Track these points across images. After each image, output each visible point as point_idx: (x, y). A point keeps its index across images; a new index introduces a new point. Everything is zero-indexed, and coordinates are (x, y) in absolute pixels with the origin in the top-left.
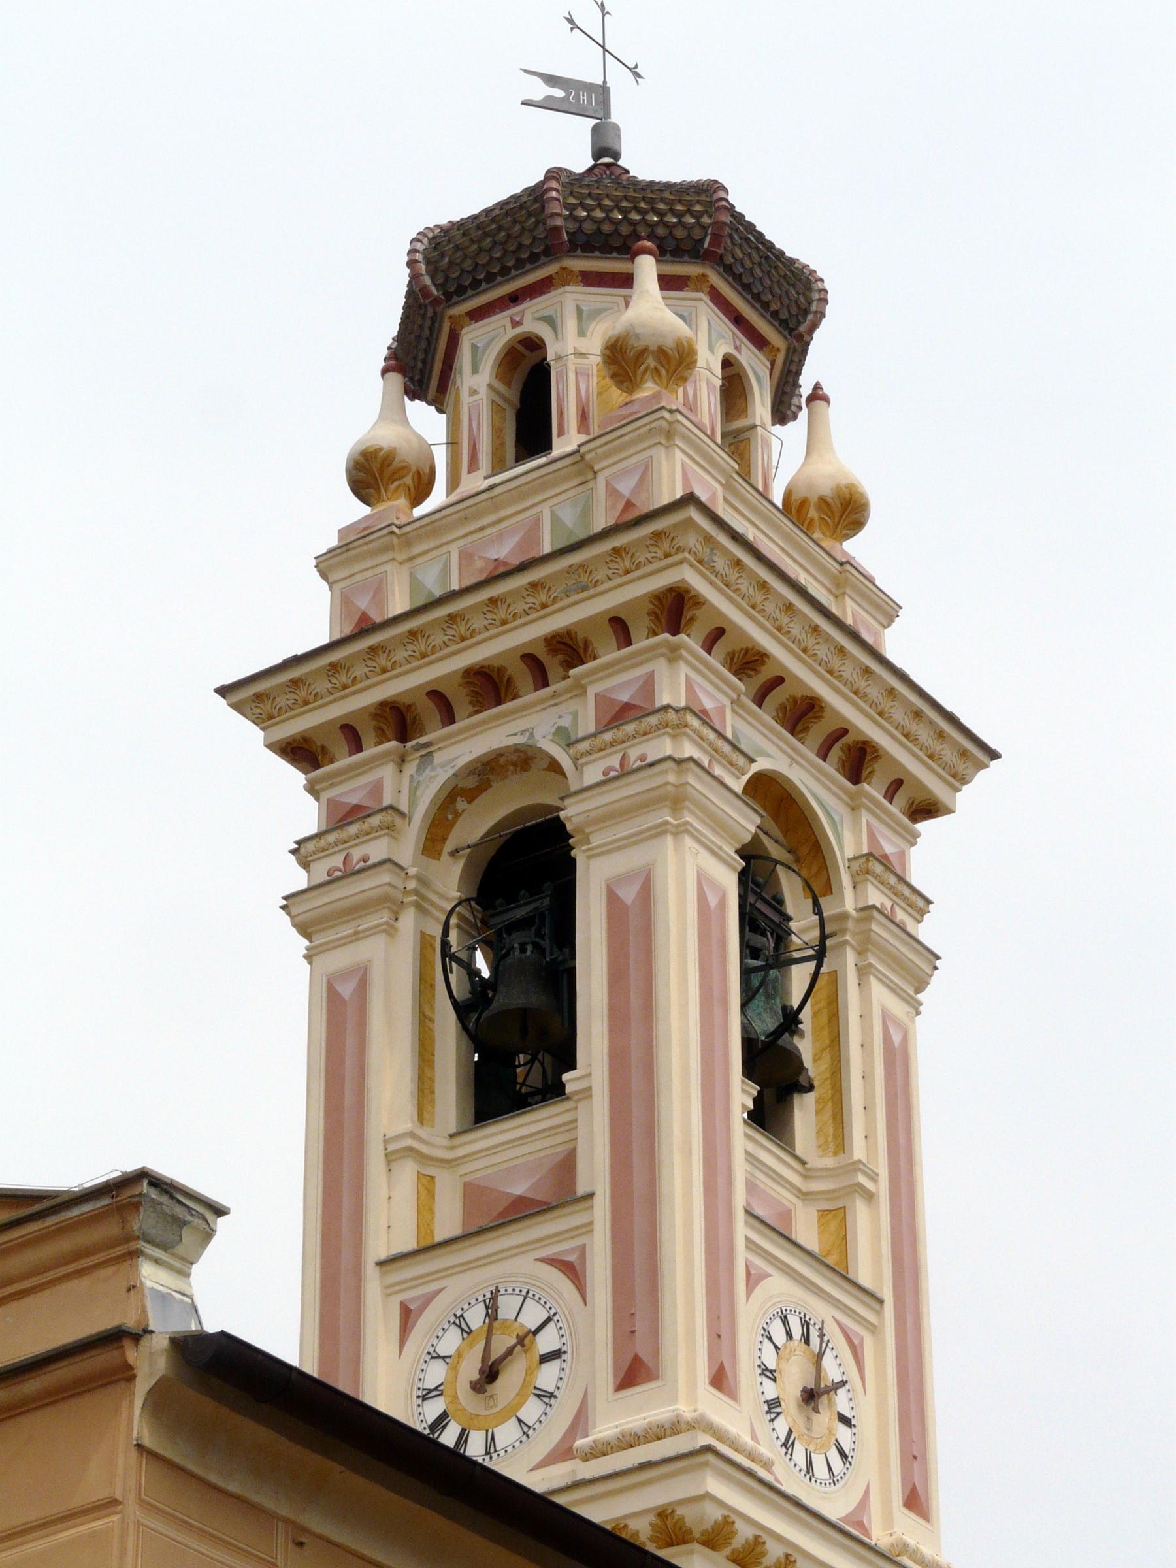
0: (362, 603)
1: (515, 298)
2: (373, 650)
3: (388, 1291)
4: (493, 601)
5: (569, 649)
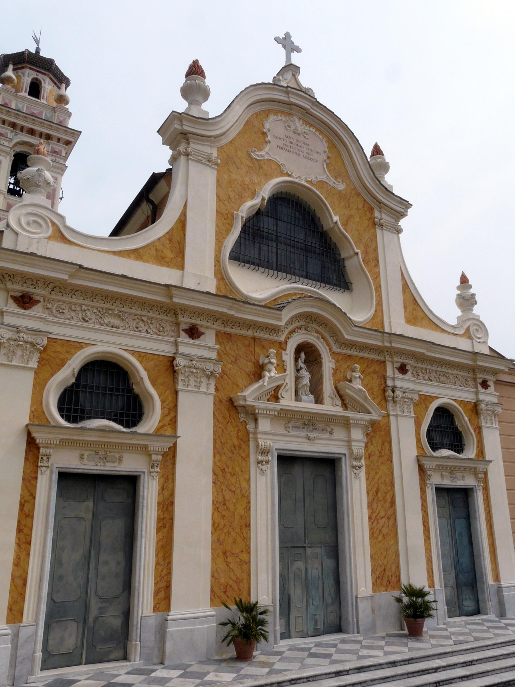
0: (7, 101)
1: (38, 71)
4: (42, 122)
5: (48, 137)
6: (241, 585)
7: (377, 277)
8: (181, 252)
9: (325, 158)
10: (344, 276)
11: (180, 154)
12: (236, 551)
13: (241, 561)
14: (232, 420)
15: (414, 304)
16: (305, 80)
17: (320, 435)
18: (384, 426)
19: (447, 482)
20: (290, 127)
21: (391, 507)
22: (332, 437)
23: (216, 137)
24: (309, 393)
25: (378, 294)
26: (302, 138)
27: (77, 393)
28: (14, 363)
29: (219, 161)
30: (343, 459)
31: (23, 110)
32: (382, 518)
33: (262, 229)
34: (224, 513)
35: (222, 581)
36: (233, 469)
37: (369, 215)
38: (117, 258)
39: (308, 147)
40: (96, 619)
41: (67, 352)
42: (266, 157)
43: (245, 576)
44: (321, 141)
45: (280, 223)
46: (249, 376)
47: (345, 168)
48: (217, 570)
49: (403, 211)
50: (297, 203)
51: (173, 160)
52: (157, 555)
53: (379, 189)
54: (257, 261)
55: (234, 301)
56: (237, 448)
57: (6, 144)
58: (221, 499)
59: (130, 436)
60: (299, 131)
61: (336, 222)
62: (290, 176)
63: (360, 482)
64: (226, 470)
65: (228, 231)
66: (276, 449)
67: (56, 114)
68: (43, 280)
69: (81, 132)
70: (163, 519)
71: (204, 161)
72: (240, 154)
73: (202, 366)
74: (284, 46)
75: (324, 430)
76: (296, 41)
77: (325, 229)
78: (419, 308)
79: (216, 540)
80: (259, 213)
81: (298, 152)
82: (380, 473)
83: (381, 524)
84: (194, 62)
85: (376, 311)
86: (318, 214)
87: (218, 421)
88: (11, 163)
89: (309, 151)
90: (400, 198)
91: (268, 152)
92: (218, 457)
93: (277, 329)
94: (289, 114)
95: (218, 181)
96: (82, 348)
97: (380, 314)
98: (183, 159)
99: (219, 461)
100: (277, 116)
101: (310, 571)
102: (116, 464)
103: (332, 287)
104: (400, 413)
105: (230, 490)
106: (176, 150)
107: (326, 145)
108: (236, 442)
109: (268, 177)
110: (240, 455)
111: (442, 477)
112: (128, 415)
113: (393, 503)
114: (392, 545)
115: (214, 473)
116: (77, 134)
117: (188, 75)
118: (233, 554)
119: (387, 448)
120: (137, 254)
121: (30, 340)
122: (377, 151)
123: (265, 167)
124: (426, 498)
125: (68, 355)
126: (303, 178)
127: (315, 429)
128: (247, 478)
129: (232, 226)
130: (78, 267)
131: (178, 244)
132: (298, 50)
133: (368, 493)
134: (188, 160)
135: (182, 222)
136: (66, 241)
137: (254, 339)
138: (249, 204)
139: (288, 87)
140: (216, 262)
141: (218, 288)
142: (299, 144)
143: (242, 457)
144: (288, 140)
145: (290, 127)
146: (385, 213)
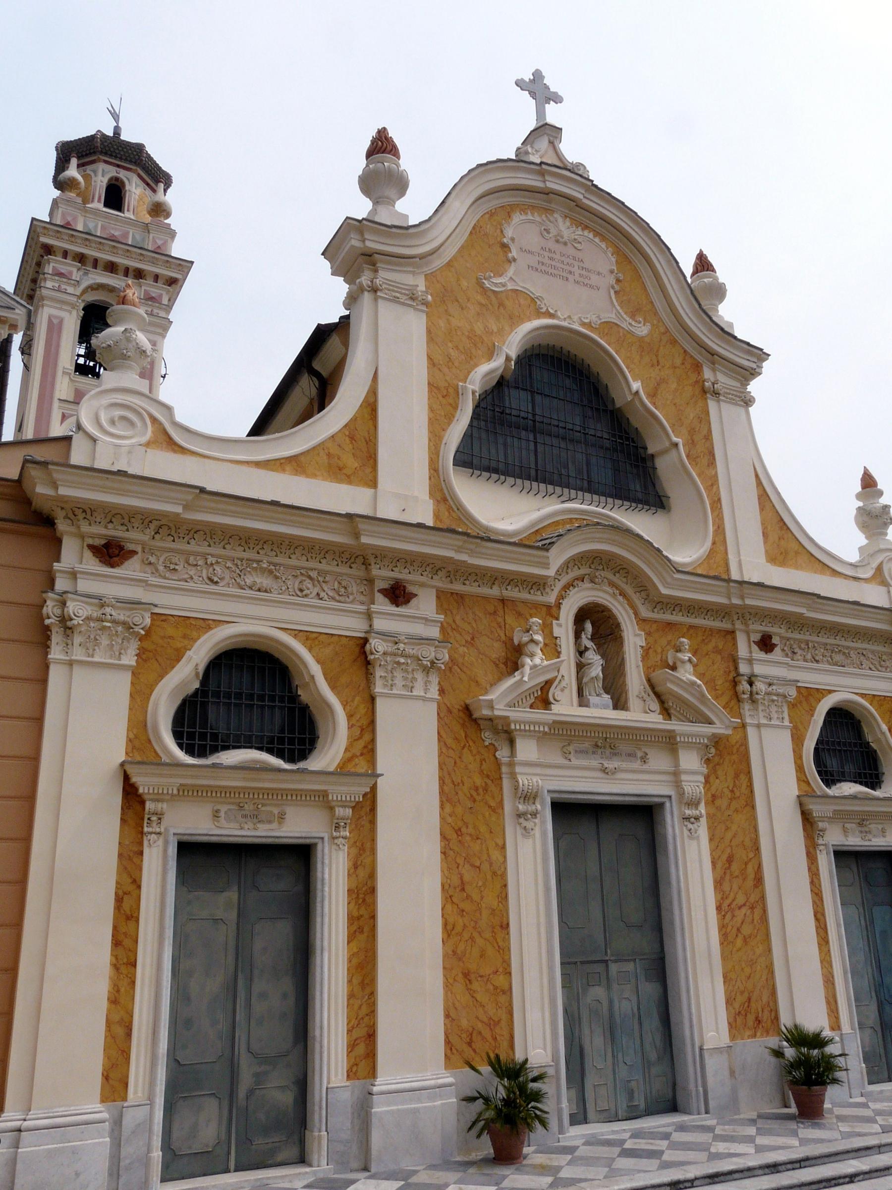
0: (69, 219)
1: (118, 166)
2: (87, 239)
3: (60, 408)
5: (139, 274)
6: (497, 1030)
7: (713, 483)
8: (370, 457)
9: (612, 281)
10: (654, 485)
11: (362, 289)
12: (486, 970)
13: (496, 988)
14: (471, 743)
15: (781, 529)
16: (571, 150)
17: (624, 765)
18: (738, 746)
19: (855, 841)
20: (548, 233)
21: (756, 886)
22: (645, 767)
23: (422, 257)
24: (602, 691)
25: (716, 513)
26: (571, 251)
27: (204, 705)
28: (97, 659)
29: (429, 297)
30: (668, 805)
31: (96, 231)
32: (740, 908)
33: (508, 411)
34: (462, 905)
35: (464, 1023)
36: (475, 827)
37: (694, 377)
38: (262, 473)
39: (581, 264)
40: (251, 1092)
41: (185, 636)
42: (510, 286)
43: (504, 1017)
44: (605, 253)
45: (538, 398)
46: (497, 665)
47: (648, 295)
48: (454, 1004)
49: (754, 366)
50: (566, 363)
51: (351, 300)
52: (350, 982)
53: (710, 330)
54: (501, 466)
55: (465, 538)
56: (481, 790)
57: (70, 290)
58: (456, 881)
59: (297, 777)
60: (566, 238)
61: (637, 392)
62: (552, 316)
63: (699, 846)
64: (464, 830)
65: (450, 418)
66: (549, 791)
67: (151, 235)
68: (140, 516)
69: (192, 263)
70: (359, 918)
71: (403, 299)
72: (464, 284)
73: (414, 651)
74: (533, 94)
76: (553, 83)
77: (619, 404)
78: (790, 535)
79: (451, 953)
80: (501, 384)
81: (565, 274)
82: (734, 827)
83: (739, 919)
84: (379, 132)
85: (714, 543)
86: (605, 379)
87: (445, 744)
88: (79, 322)
89: (584, 272)
90: (748, 344)
91: (513, 278)
92: (448, 808)
93: (542, 582)
94: (547, 211)
95: (429, 331)
96: (210, 628)
97: (722, 548)
98: (367, 297)
99: (450, 815)
100: (527, 214)
102: (275, 825)
103: (634, 505)
104: (764, 721)
105: (473, 866)
106: (355, 284)
107: (614, 260)
108: (479, 781)
109: (515, 320)
110: (486, 803)
111: (845, 831)
112: (291, 741)
113: (759, 880)
114: (760, 956)
115: (444, 837)
116: (185, 266)
117: (370, 154)
118: (481, 976)
120: (295, 464)
121: (122, 618)
122: (703, 264)
123: (509, 304)
124: (818, 870)
125: (186, 642)
126: (575, 318)
127: (615, 754)
128: (500, 843)
129: (455, 408)
130: (198, 491)
131: (364, 444)
132: (557, 99)
133: (714, 863)
134: (376, 299)
135: (370, 407)
136: (176, 448)
137: (503, 601)
138: (484, 368)
139: (542, 163)
140: (432, 472)
141: (437, 516)
142: (566, 261)
143: (490, 807)
144: (546, 254)
145: (548, 233)
146: (722, 372)
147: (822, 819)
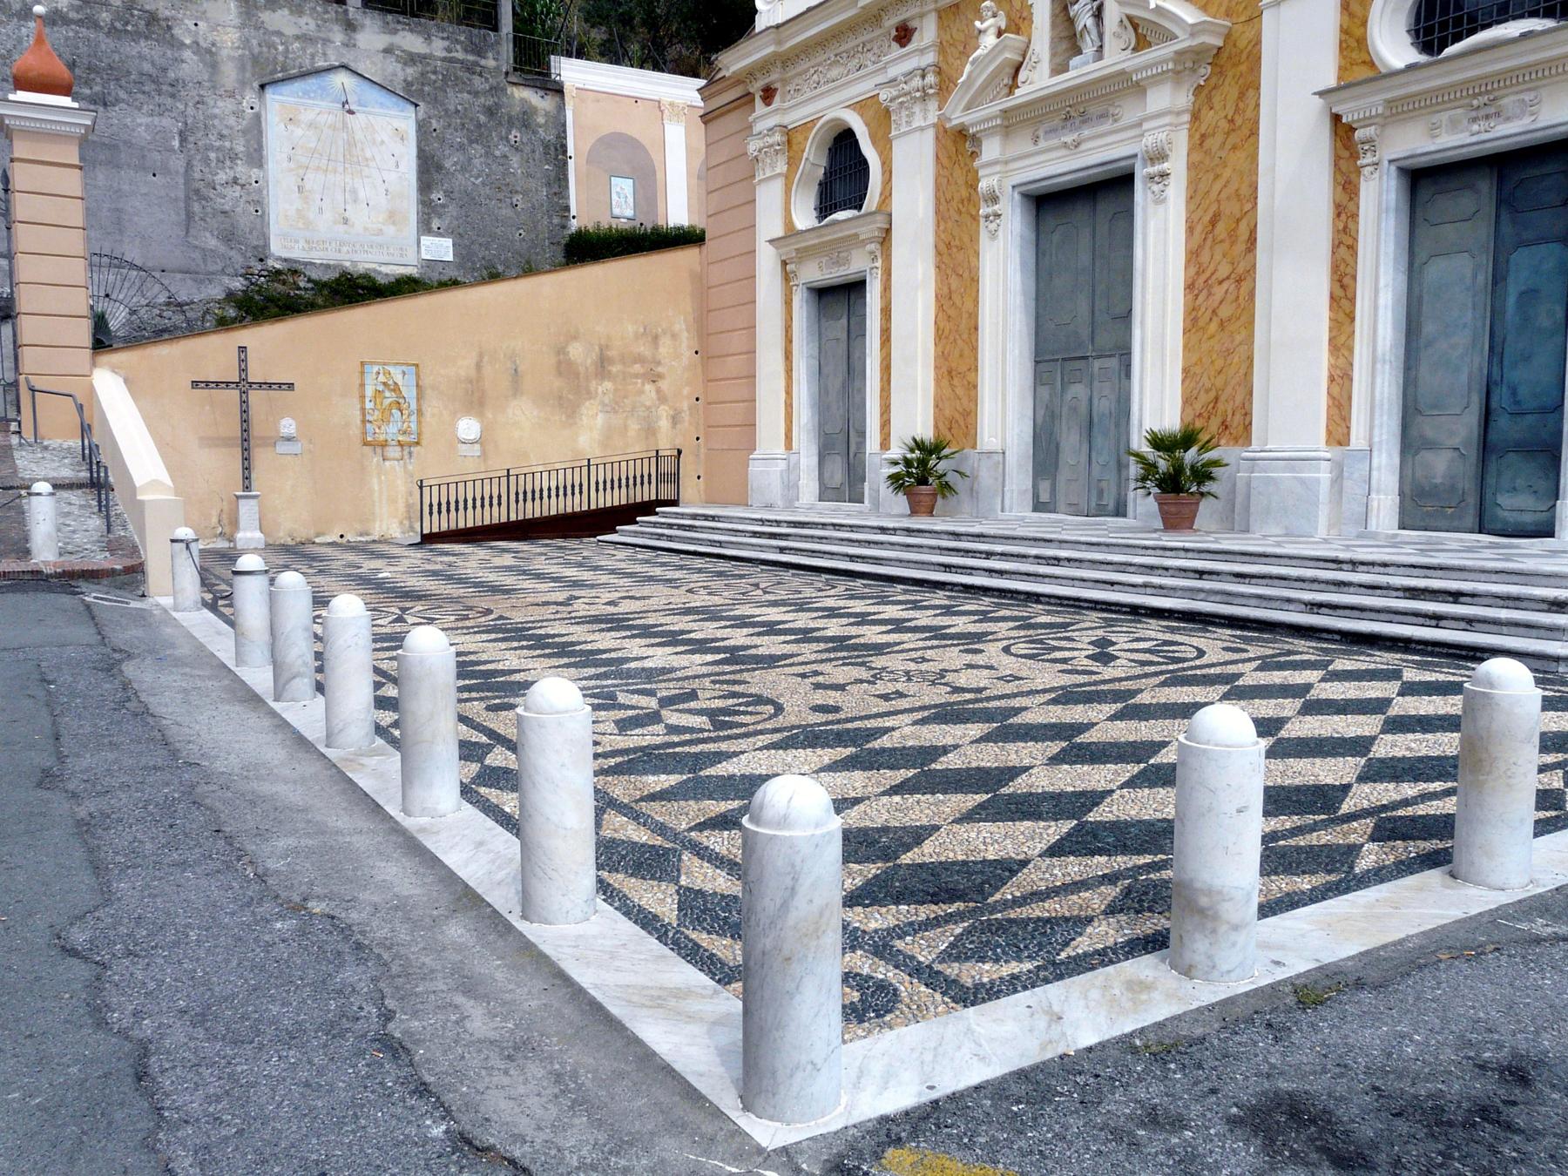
12: (963, 368)
32: (1220, 283)
34: (950, 312)
35: (947, 413)
58: (946, 290)
59: (829, 230)
75: (1103, 116)
82: (1227, 173)
101: (1095, 402)
111: (1433, 131)
115: (938, 253)
119: (1251, 107)
127: (1084, 122)
133: (1190, 230)
147: (1367, 122)
